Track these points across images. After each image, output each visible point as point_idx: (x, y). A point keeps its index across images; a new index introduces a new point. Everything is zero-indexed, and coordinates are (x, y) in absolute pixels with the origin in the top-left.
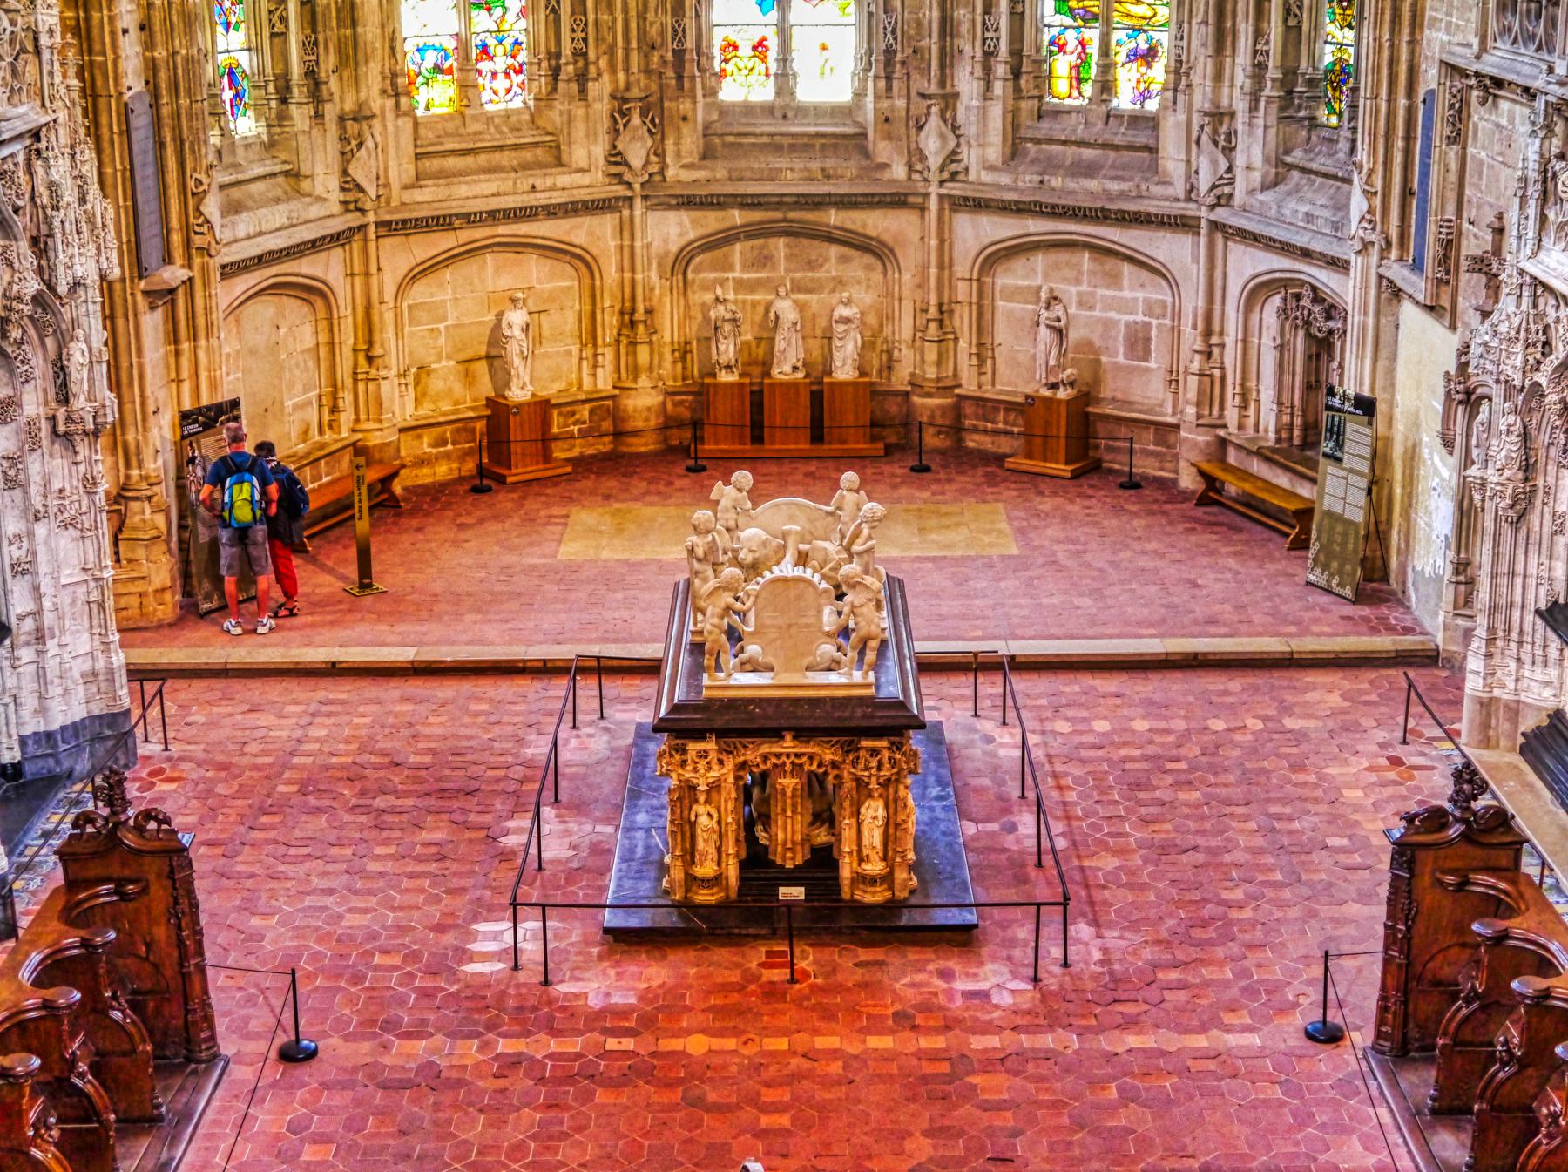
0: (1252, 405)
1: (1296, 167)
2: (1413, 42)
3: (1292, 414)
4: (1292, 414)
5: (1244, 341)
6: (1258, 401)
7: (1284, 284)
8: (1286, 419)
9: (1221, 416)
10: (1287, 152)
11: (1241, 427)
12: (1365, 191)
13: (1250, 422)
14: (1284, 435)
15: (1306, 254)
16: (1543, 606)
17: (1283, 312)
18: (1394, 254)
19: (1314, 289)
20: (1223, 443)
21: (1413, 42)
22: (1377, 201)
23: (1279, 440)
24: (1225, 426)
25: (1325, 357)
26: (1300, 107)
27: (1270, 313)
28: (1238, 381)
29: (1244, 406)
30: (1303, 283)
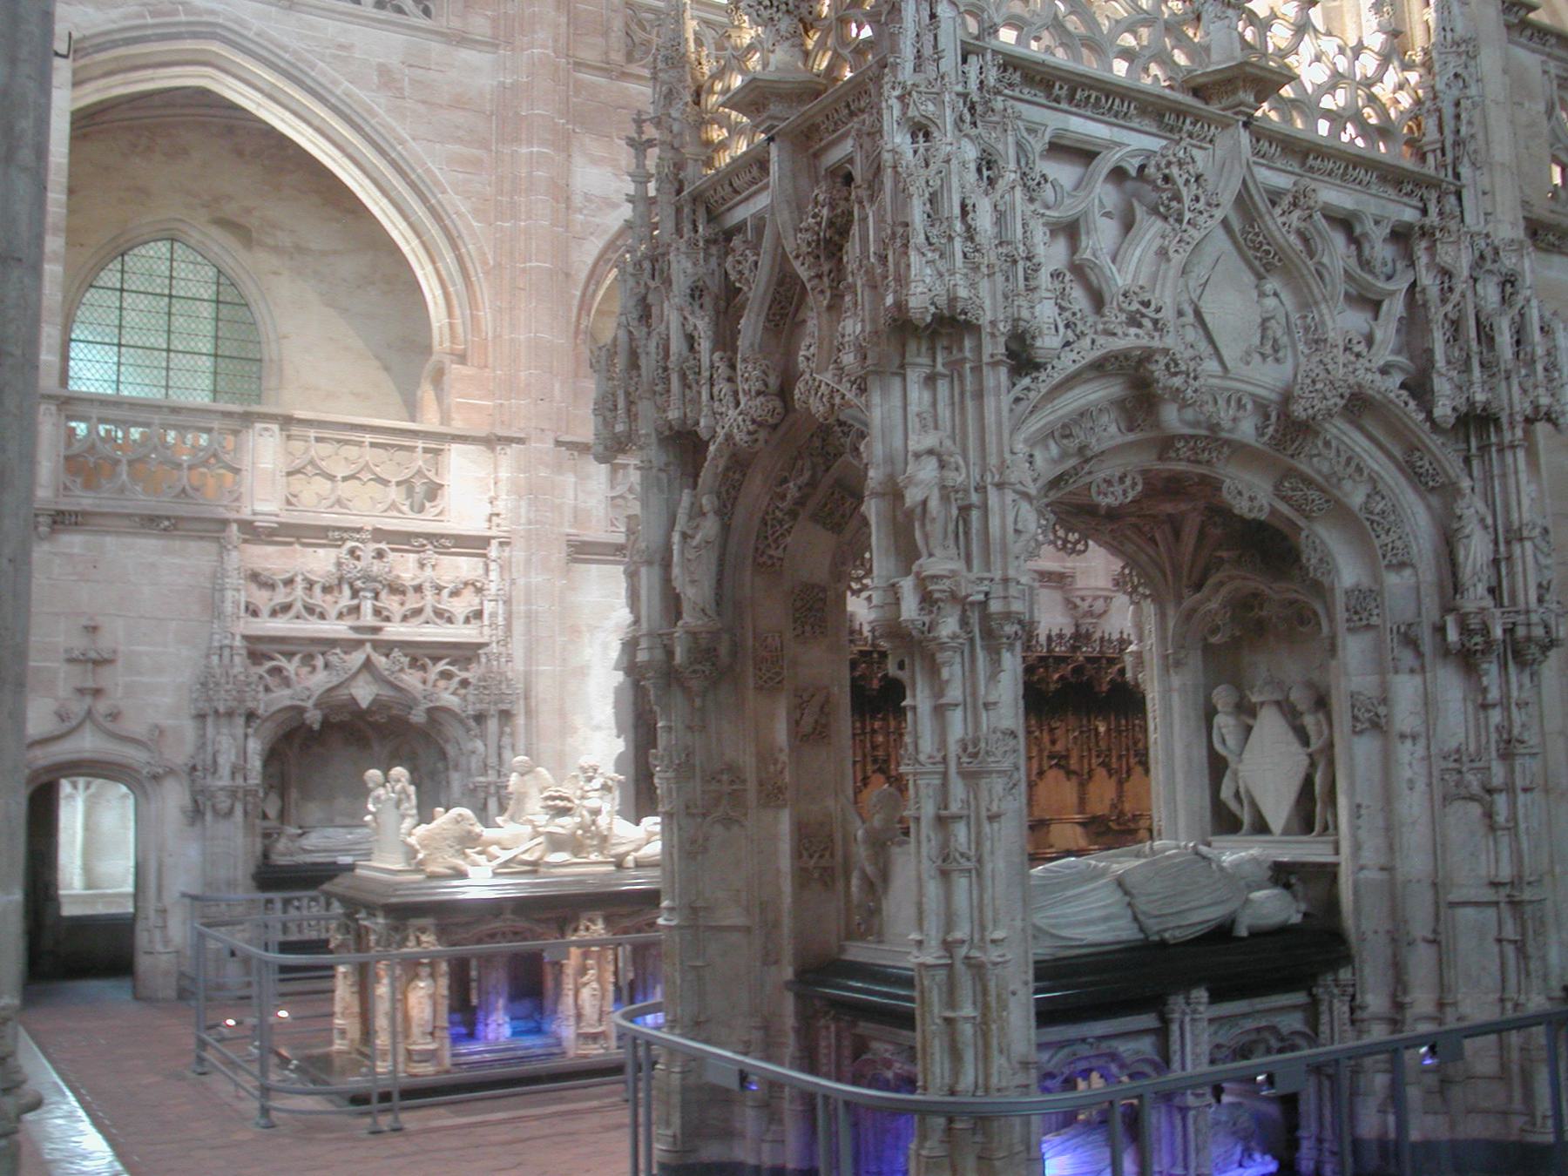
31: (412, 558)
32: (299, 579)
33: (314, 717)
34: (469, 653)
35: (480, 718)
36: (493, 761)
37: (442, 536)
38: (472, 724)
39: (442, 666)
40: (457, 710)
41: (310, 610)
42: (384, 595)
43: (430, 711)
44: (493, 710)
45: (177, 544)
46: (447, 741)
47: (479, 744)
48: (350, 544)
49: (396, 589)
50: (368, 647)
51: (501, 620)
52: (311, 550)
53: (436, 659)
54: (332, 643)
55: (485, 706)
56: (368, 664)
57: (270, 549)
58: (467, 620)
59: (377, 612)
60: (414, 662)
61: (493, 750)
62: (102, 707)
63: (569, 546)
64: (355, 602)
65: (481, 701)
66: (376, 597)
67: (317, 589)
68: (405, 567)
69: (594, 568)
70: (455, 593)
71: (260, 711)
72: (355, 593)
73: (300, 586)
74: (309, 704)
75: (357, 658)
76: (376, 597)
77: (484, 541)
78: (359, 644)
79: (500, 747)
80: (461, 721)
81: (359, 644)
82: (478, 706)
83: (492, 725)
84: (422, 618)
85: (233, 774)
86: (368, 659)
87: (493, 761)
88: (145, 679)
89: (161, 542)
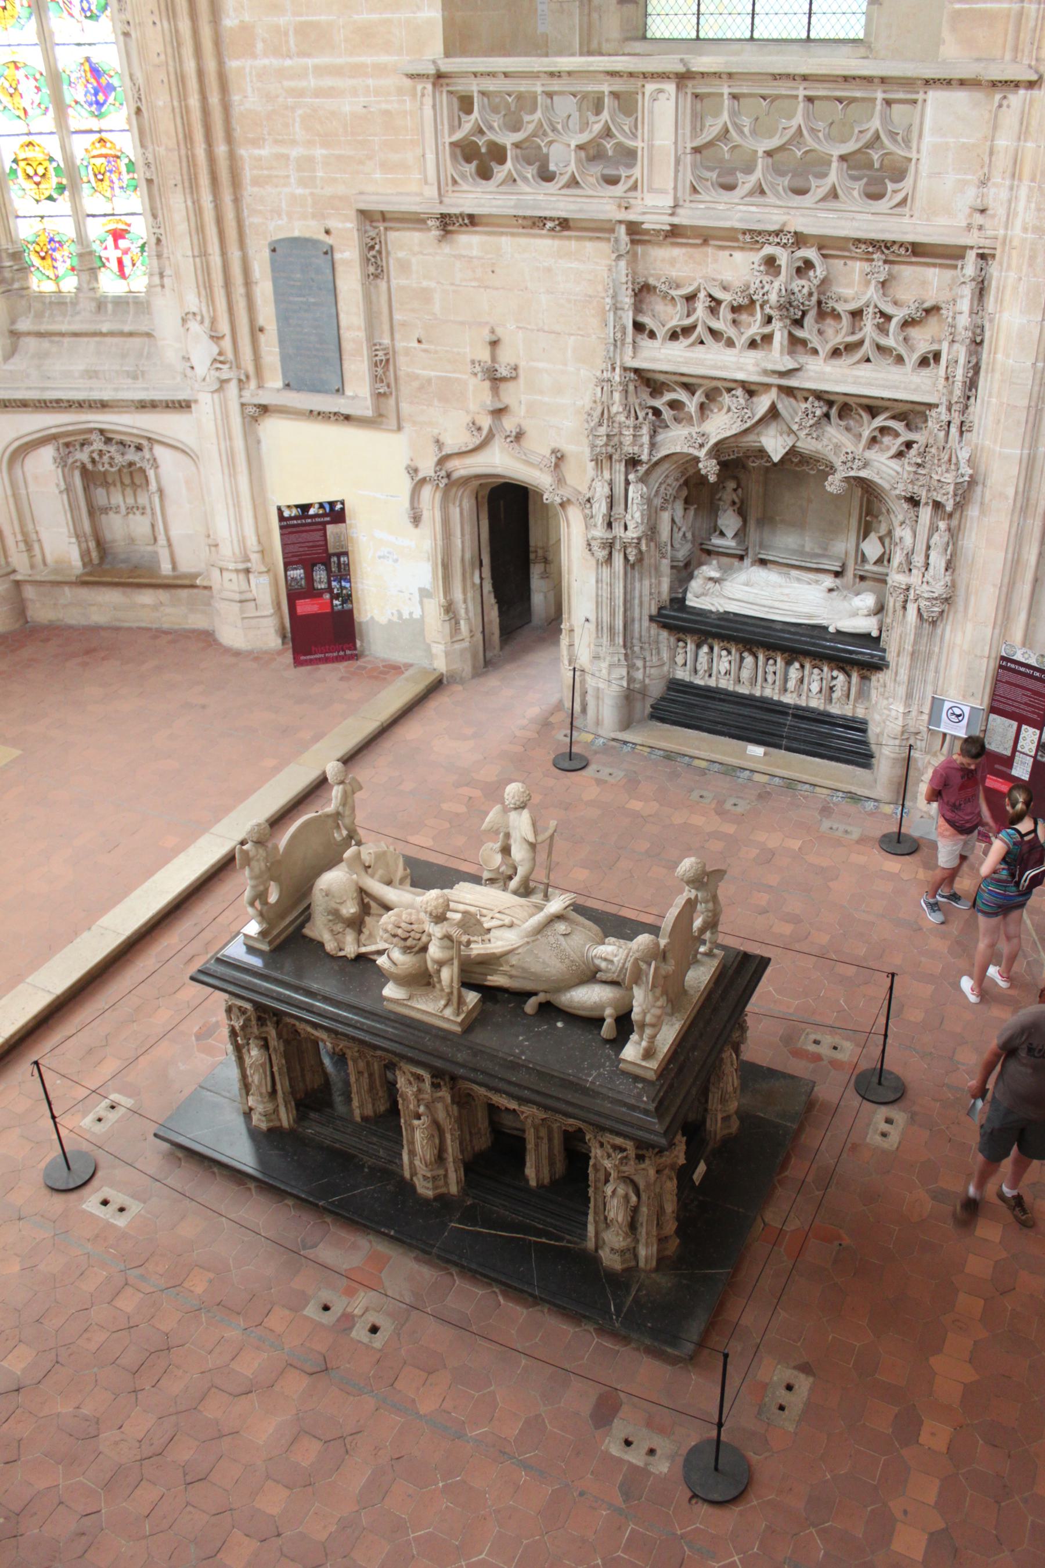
0: (36, 546)
1: (29, 334)
2: (237, 201)
3: (87, 541)
4: (87, 541)
5: (14, 495)
6: (39, 540)
7: (54, 437)
8: (84, 545)
9: (7, 563)
10: (13, 322)
11: (32, 566)
12: (212, 337)
13: (39, 557)
14: (86, 560)
15: (104, 405)
16: (654, 612)
17: (62, 462)
18: (253, 384)
19: (102, 432)
20: (17, 584)
21: (237, 201)
22: (227, 344)
23: (84, 565)
24: (14, 571)
25: (92, 486)
26: (13, 280)
27: (44, 462)
28: (17, 530)
29: (29, 548)
30: (91, 431)
32: (702, 295)
33: (709, 468)
36: (918, 559)
39: (880, 421)
42: (809, 320)
45: (573, 244)
50: (773, 393)
52: (727, 253)
56: (773, 413)
61: (921, 547)
62: (509, 424)
66: (799, 323)
67: (724, 311)
71: (644, 457)
73: (701, 305)
74: (702, 454)
75: (763, 404)
79: (928, 548)
83: (926, 513)
84: (859, 354)
85: (610, 525)
87: (918, 559)
88: (546, 399)
89: (557, 243)
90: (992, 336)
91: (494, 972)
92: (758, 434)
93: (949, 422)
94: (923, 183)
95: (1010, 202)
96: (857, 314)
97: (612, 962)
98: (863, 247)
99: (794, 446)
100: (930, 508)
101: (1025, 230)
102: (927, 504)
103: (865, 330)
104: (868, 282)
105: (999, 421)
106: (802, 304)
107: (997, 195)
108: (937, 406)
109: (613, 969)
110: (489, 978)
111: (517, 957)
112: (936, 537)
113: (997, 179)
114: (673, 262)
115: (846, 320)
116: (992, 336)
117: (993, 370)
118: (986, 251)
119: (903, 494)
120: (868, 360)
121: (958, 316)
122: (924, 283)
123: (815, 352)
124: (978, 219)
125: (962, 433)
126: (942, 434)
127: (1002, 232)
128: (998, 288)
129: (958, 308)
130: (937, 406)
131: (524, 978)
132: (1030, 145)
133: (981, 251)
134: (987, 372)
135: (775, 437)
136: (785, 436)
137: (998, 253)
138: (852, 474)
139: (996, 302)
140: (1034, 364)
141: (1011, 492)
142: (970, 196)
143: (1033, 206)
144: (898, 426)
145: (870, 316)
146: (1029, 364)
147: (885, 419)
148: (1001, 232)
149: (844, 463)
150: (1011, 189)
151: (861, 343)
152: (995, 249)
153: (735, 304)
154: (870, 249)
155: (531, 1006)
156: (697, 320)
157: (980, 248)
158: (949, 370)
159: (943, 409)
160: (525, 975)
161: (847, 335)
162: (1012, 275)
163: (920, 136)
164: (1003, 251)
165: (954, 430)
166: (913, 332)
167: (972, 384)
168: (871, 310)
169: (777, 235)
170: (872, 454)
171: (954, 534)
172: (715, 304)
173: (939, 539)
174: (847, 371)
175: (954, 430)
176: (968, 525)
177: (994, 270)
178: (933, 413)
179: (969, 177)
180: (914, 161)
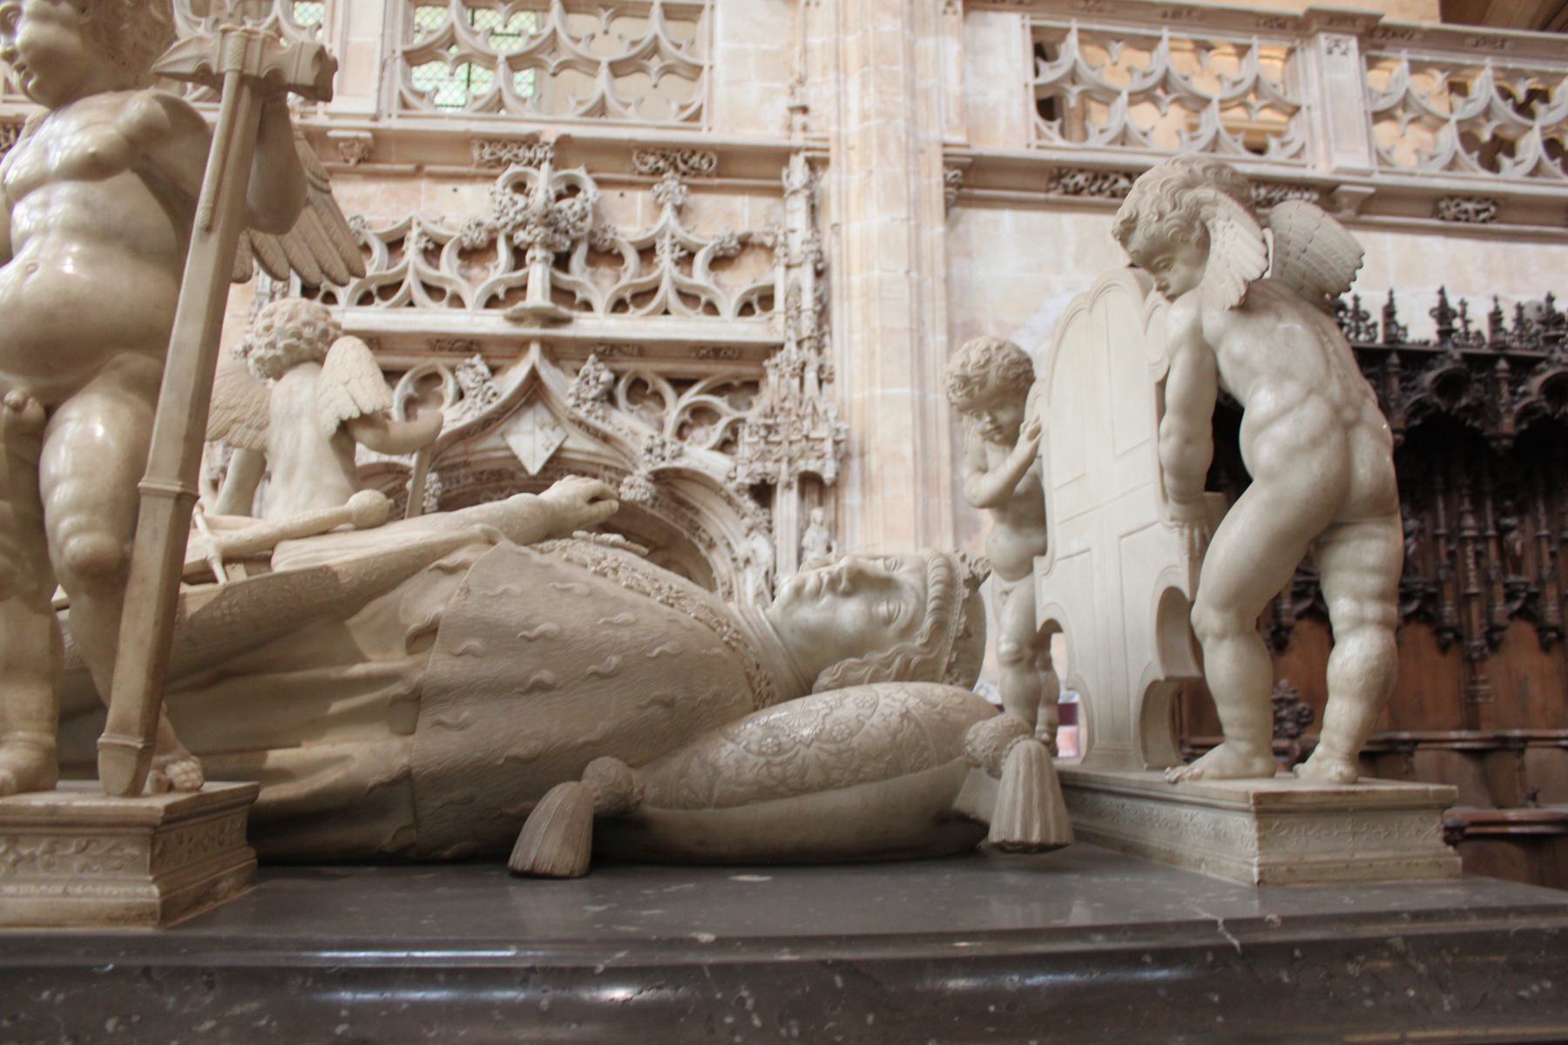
31: (640, 198)
32: (413, 234)
34: (749, 371)
35: (763, 493)
37: (694, 150)
38: (750, 504)
39: (691, 396)
40: (720, 478)
41: (434, 291)
43: (658, 477)
44: (783, 473)
46: (711, 545)
47: (760, 544)
48: (513, 169)
49: (604, 255)
50: (534, 354)
51: (807, 301)
53: (681, 384)
54: (469, 345)
55: (770, 467)
57: (373, 189)
58: (746, 309)
59: (561, 293)
60: (639, 390)
63: (947, 165)
64: (520, 273)
65: (763, 457)
66: (561, 261)
67: (448, 257)
68: (631, 216)
69: (1007, 220)
70: (720, 261)
72: (519, 256)
73: (412, 252)
75: (515, 377)
76: (561, 261)
77: (781, 156)
78: (519, 346)
80: (729, 501)
81: (521, 345)
82: (758, 467)
83: (787, 503)
86: (534, 376)
90: (840, 254)
91: (309, 708)
92: (502, 435)
93: (804, 365)
94: (721, 92)
95: (838, 95)
96: (647, 252)
97: (884, 585)
98: (651, 160)
99: (560, 449)
100: (793, 495)
101: (865, 117)
102: (789, 486)
103: (662, 266)
104: (661, 207)
105: (872, 354)
106: (574, 226)
107: (818, 94)
108: (781, 347)
109: (905, 607)
110: (277, 757)
111: (449, 584)
112: (811, 534)
113: (815, 78)
114: (365, 202)
115: (631, 258)
116: (840, 254)
117: (849, 297)
118: (818, 154)
119: (748, 481)
120: (666, 312)
121: (790, 236)
122: (731, 215)
123: (587, 306)
124: (799, 119)
125: (820, 382)
126: (796, 382)
127: (833, 128)
128: (839, 193)
129: (790, 226)
130: (781, 347)
131: (495, 690)
132: (851, 39)
133: (810, 154)
134: (841, 297)
135: (532, 432)
136: (548, 430)
137: (833, 155)
138: (663, 465)
139: (840, 207)
140: (908, 272)
141: (907, 450)
142: (784, 102)
143: (872, 90)
144: (719, 403)
145: (667, 248)
146: (901, 271)
147: (700, 393)
148: (833, 128)
149: (650, 451)
150: (838, 81)
151: (655, 290)
152: (827, 150)
153: (466, 243)
154: (661, 164)
155: (550, 832)
156: (405, 271)
157: (808, 149)
158: (791, 299)
159: (791, 346)
160: (499, 667)
161: (633, 276)
162: (855, 179)
163: (711, 44)
164: (839, 150)
165: (811, 376)
166: (726, 276)
167: (823, 313)
168: (667, 241)
169: (530, 147)
170: (686, 446)
171: (834, 528)
172: (432, 252)
173: (815, 536)
174: (641, 323)
175: (811, 376)
176: (848, 520)
177: (829, 179)
178: (779, 357)
179: (778, 85)
180: (706, 69)
